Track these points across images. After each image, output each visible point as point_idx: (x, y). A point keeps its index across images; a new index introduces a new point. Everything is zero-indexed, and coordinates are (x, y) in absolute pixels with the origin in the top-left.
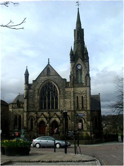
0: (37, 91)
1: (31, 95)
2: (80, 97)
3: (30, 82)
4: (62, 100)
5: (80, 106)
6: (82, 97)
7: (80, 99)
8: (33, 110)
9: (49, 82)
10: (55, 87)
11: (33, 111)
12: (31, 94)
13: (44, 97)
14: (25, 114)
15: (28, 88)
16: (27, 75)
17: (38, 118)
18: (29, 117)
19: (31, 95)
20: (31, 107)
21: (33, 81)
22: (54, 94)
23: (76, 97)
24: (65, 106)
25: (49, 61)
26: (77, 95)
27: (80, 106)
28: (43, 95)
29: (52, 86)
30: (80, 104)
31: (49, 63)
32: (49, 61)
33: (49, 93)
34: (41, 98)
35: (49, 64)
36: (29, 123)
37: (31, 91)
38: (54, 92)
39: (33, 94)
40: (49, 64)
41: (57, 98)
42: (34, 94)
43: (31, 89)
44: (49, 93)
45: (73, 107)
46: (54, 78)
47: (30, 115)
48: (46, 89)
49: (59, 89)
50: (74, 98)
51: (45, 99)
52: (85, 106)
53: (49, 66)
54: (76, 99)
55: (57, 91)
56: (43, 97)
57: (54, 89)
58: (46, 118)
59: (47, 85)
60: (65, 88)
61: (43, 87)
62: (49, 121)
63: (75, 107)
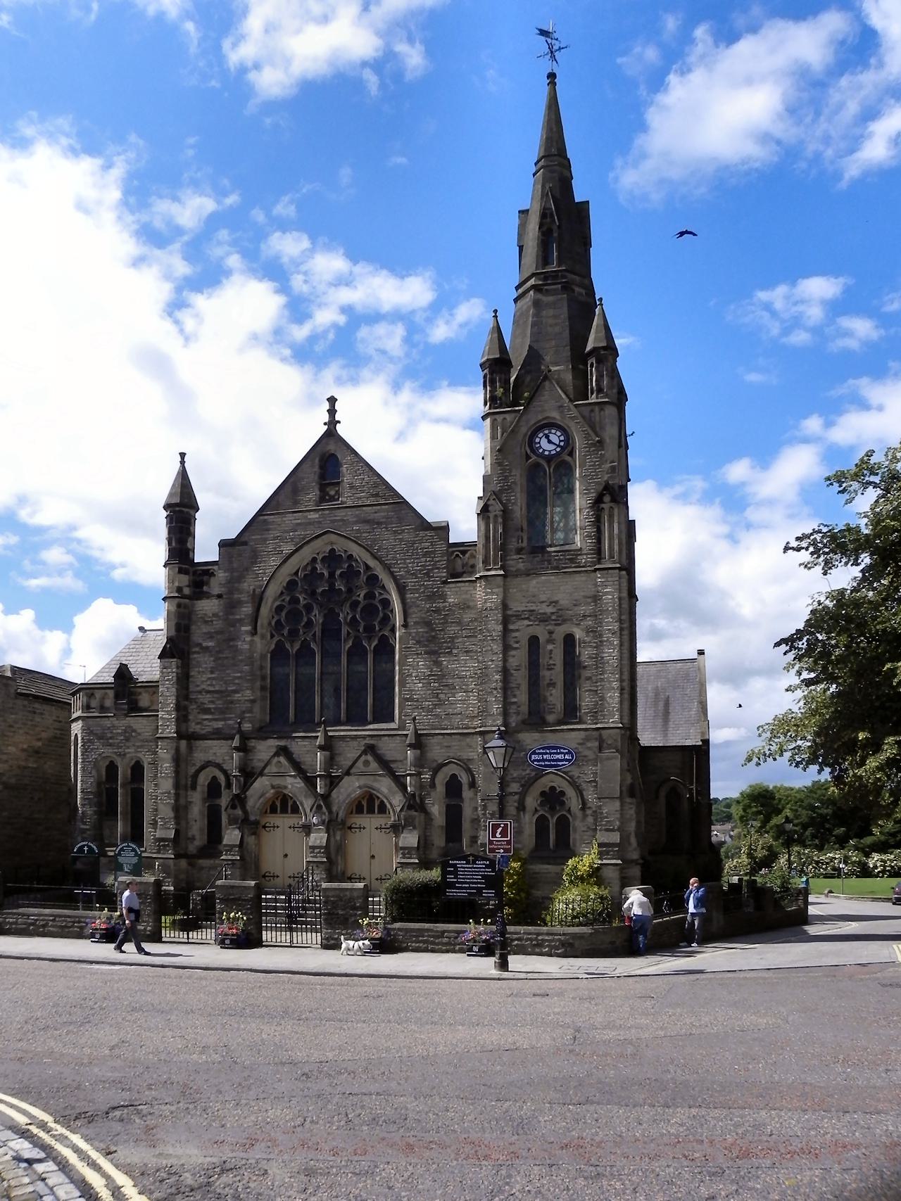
0: (247, 609)
1: (210, 636)
2: (550, 641)
3: (205, 550)
4: (421, 665)
5: (555, 697)
6: (569, 640)
7: (554, 654)
8: (220, 724)
9: (332, 550)
10: (373, 580)
11: (218, 735)
12: (205, 629)
13: (297, 646)
14: (165, 753)
15: (187, 591)
16: (182, 511)
17: (249, 775)
18: (192, 770)
19: (210, 636)
20: (207, 711)
21: (224, 544)
22: (369, 629)
23: (524, 642)
24: (441, 703)
25: (332, 412)
26: (523, 630)
27: (555, 697)
28: (293, 634)
29: (351, 574)
30: (552, 684)
31: (332, 423)
32: (332, 412)
33: (331, 617)
34: (279, 654)
35: (331, 433)
36: (197, 810)
37: (207, 607)
38: (370, 611)
39: (218, 624)
40: (331, 433)
41: (385, 649)
42: (233, 624)
43: (207, 596)
44: (331, 617)
45: (496, 708)
46: (367, 522)
47: (199, 757)
48: (313, 593)
49: (402, 590)
50: (506, 648)
51: (305, 654)
52: (586, 701)
53: (332, 447)
54: (519, 658)
55: (386, 603)
56: (288, 646)
57: (370, 596)
58: (310, 782)
59: (318, 566)
60: (445, 582)
61: (291, 585)
62: (326, 797)
63: (513, 709)
